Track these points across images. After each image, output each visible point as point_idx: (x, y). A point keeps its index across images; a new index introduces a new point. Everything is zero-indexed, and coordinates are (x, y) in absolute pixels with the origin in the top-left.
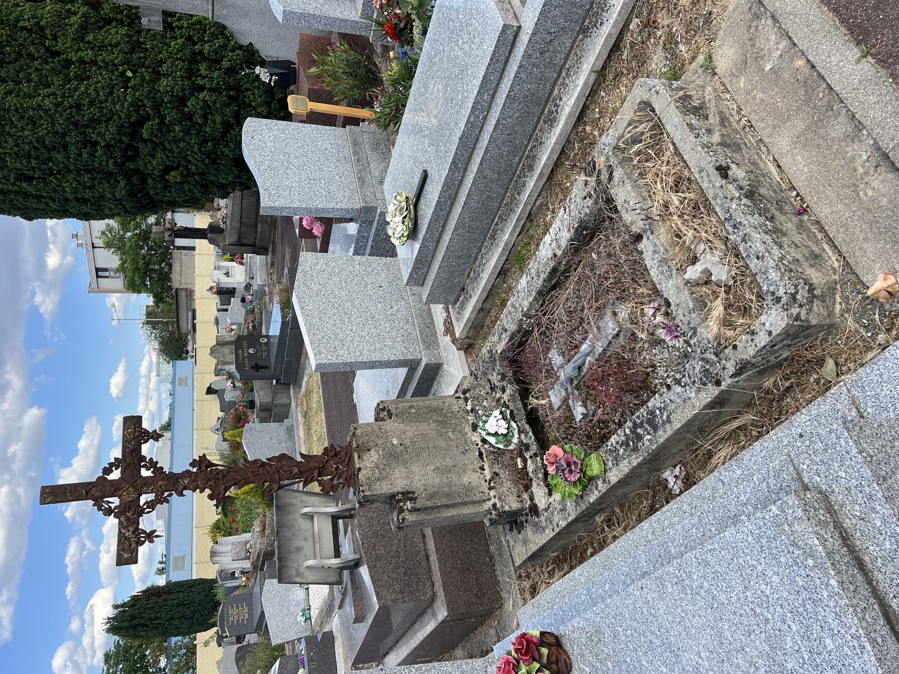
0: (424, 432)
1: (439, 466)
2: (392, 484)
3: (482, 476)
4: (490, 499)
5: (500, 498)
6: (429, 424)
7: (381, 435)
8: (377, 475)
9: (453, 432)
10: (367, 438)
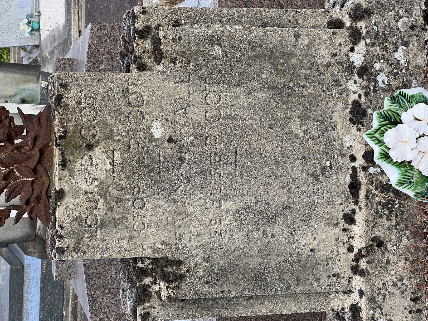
0: (233, 113)
1: (252, 205)
2: (132, 238)
3: (344, 237)
4: (350, 292)
5: (372, 300)
6: (250, 92)
7: (127, 110)
8: (100, 213)
9: (304, 118)
10: (91, 115)
